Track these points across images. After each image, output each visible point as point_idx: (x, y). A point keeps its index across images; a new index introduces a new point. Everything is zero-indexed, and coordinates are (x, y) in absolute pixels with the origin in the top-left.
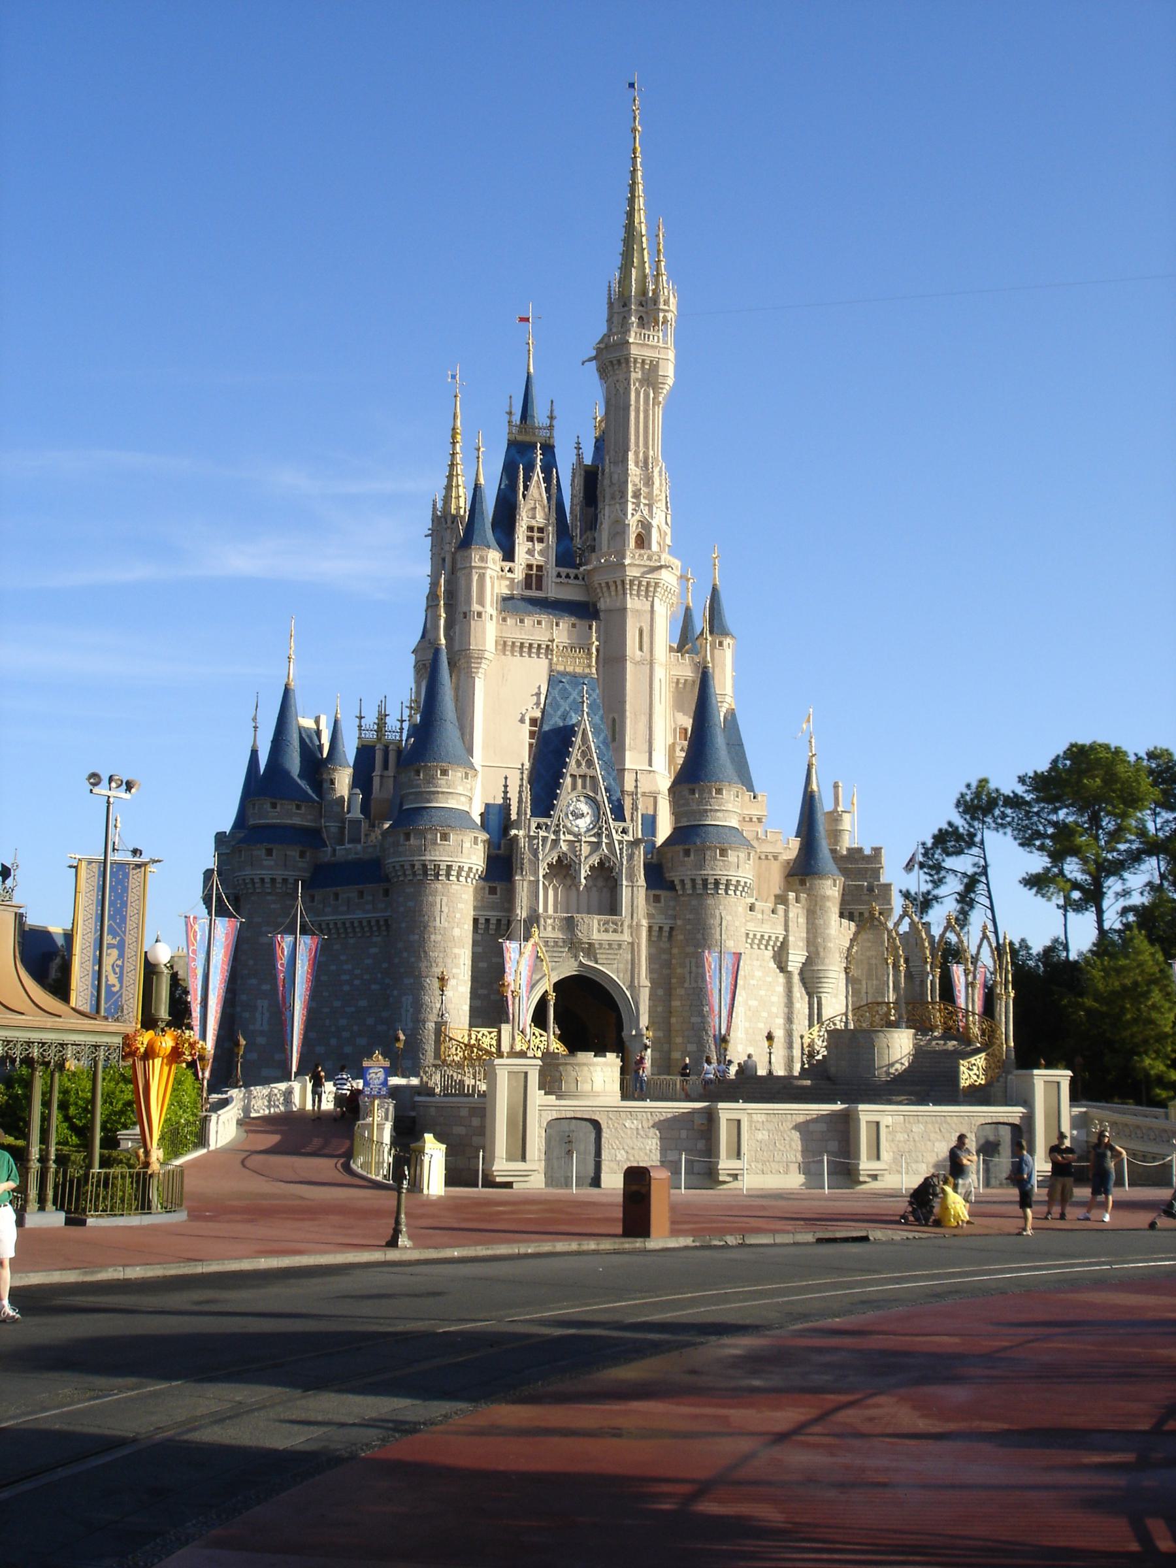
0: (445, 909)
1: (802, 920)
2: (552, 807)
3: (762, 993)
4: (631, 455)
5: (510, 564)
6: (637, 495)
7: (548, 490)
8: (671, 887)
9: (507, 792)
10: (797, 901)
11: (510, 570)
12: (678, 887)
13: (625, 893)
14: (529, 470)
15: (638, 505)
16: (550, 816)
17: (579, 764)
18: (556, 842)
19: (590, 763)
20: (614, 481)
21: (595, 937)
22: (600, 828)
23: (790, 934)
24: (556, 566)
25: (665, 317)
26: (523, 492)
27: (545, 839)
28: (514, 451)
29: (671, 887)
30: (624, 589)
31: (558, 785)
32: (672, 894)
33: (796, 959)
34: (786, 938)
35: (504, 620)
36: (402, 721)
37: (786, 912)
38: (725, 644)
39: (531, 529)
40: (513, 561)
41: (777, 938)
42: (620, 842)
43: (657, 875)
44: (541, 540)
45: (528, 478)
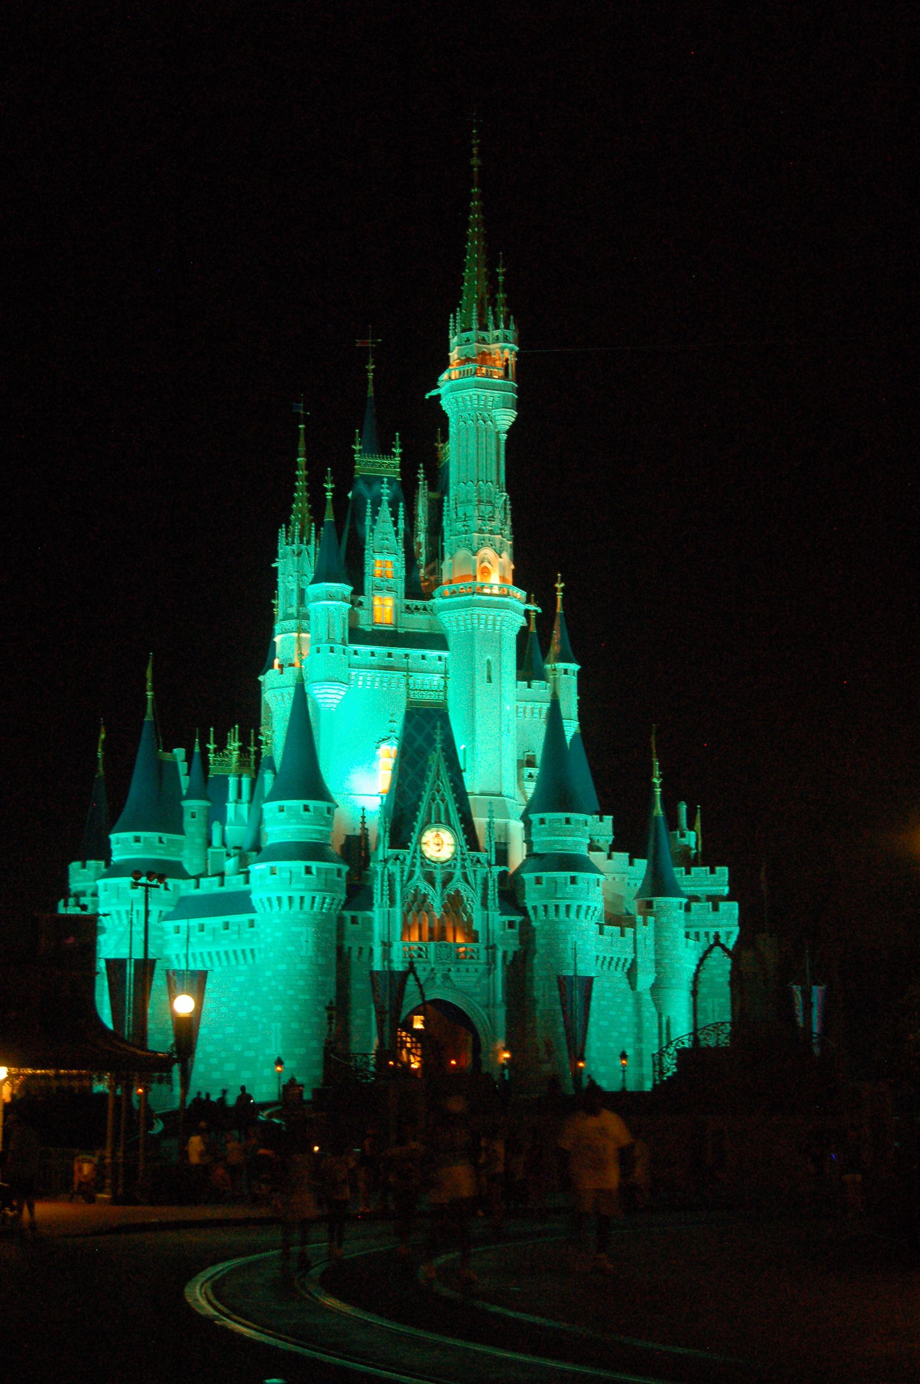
1: (650, 942)
3: (612, 1013)
5: (361, 598)
7: (395, 524)
9: (365, 823)
10: (645, 923)
12: (531, 913)
14: (377, 502)
16: (408, 848)
20: (460, 514)
23: (639, 955)
26: (371, 526)
33: (645, 980)
37: (635, 933)
41: (626, 960)
45: (375, 513)
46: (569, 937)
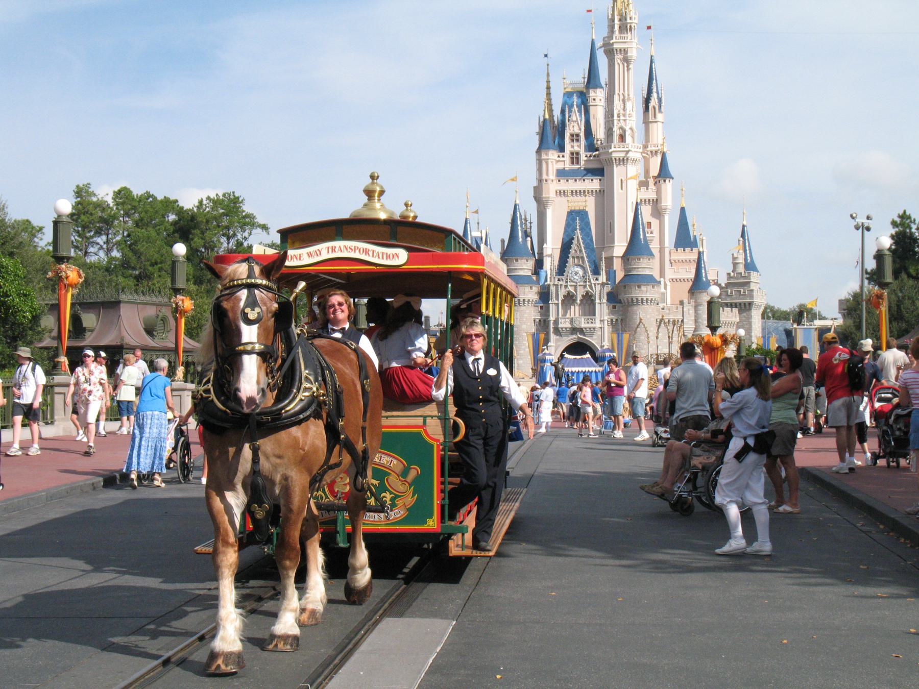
0: (519, 317)
1: (692, 312)
2: (564, 271)
4: (616, 97)
5: (563, 153)
6: (619, 116)
8: (620, 302)
11: (563, 156)
13: (598, 307)
15: (619, 120)
17: (576, 251)
18: (566, 286)
19: (581, 251)
21: (583, 326)
22: (586, 279)
23: (685, 318)
24: (585, 151)
25: (630, 26)
27: (561, 285)
28: (566, 98)
29: (620, 302)
30: (613, 163)
31: (567, 262)
32: (620, 305)
34: (682, 321)
35: (559, 181)
36: (531, 223)
37: (683, 308)
38: (667, 181)
39: (572, 135)
40: (564, 152)
42: (595, 285)
43: (613, 298)
44: (577, 140)
45: (570, 111)
46: (638, 313)
